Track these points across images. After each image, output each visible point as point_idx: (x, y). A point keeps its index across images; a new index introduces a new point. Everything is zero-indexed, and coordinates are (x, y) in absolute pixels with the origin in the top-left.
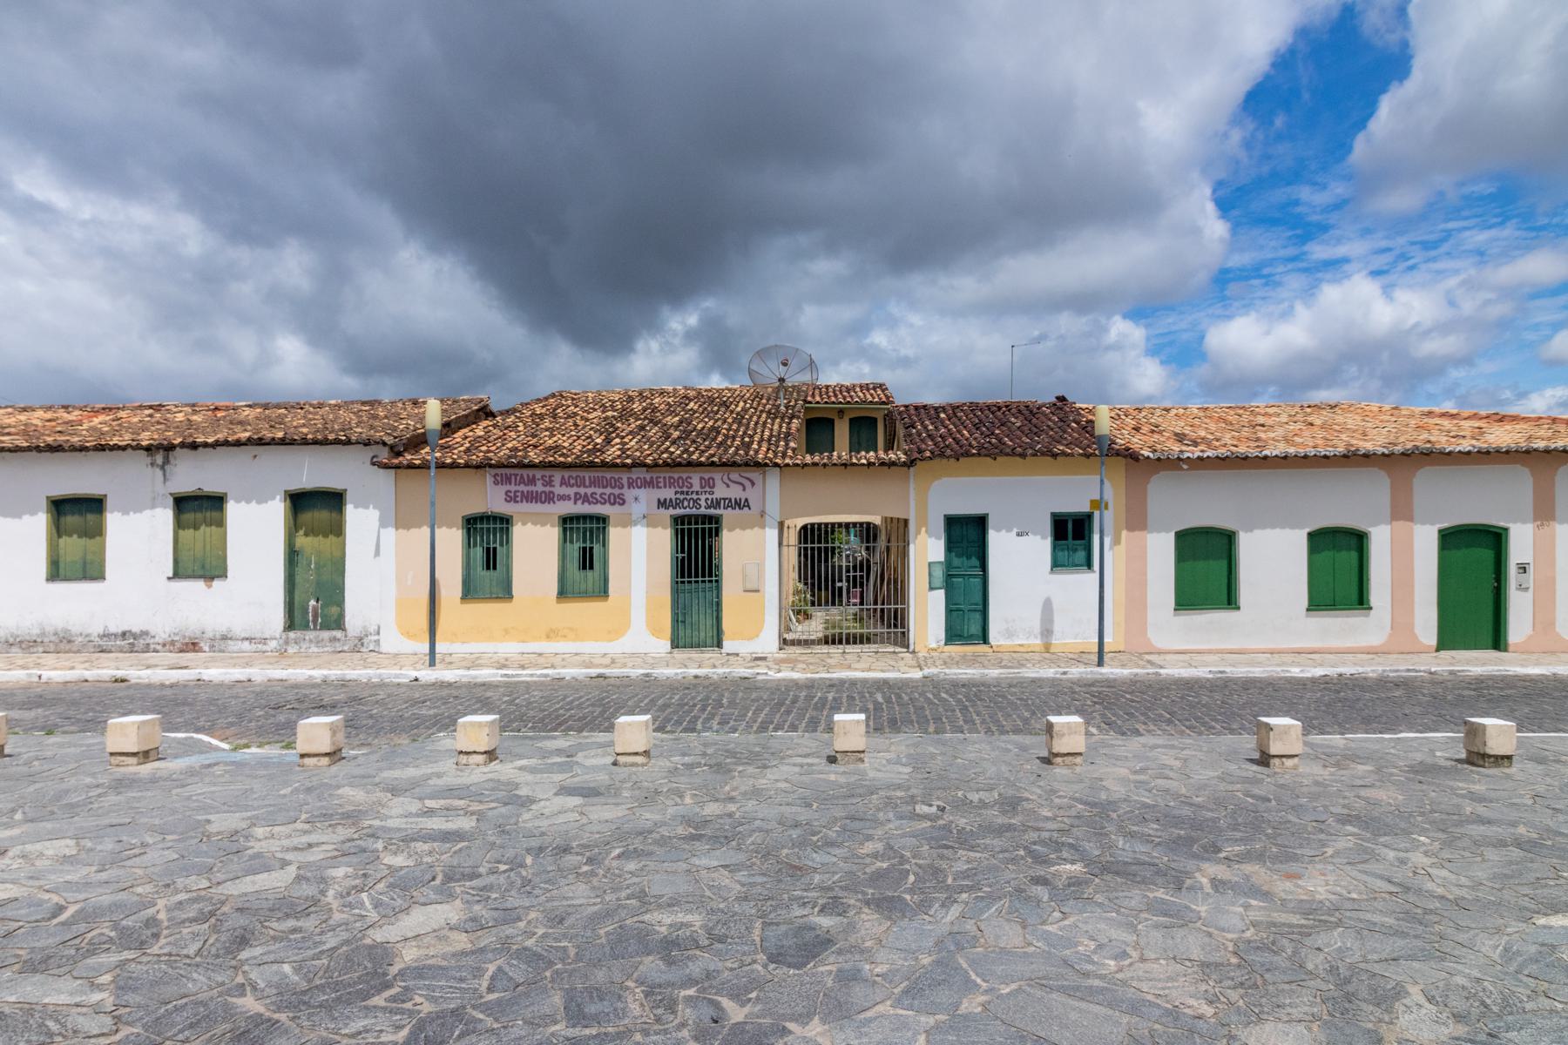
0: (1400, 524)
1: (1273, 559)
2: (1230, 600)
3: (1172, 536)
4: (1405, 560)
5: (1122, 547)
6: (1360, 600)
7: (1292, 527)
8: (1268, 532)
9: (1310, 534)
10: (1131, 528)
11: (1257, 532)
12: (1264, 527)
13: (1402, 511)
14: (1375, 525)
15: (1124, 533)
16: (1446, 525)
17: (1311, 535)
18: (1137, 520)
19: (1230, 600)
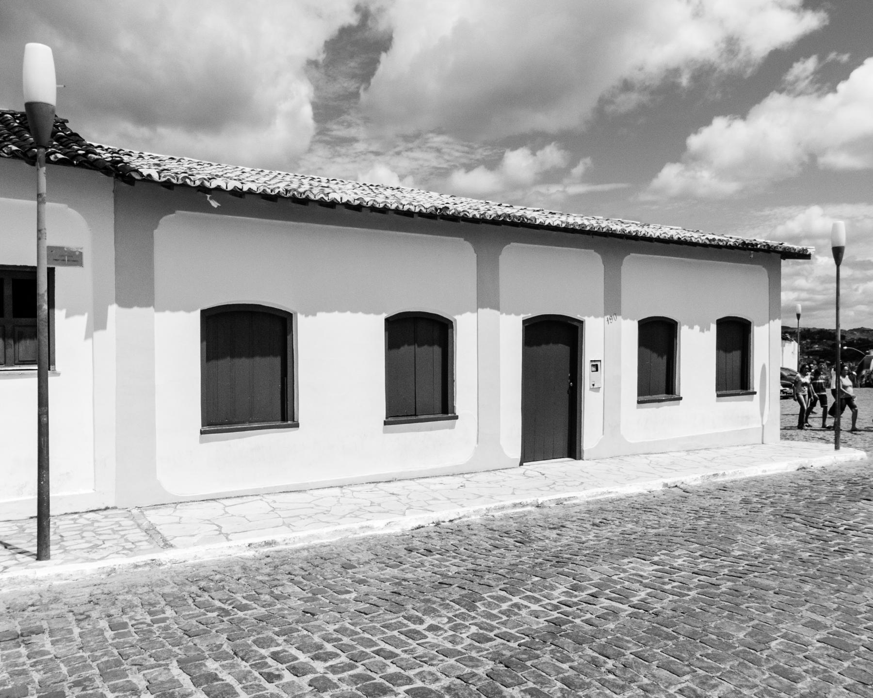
0: (487, 313)
1: (340, 355)
2: (284, 414)
3: (197, 315)
4: (489, 357)
5: (107, 337)
6: (444, 408)
7: (367, 312)
8: (336, 316)
9: (387, 320)
10: (125, 300)
11: (321, 315)
12: (329, 310)
13: (487, 298)
14: (460, 313)
15: (113, 309)
16: (530, 315)
17: (391, 323)
18: (135, 286)
19: (284, 414)
